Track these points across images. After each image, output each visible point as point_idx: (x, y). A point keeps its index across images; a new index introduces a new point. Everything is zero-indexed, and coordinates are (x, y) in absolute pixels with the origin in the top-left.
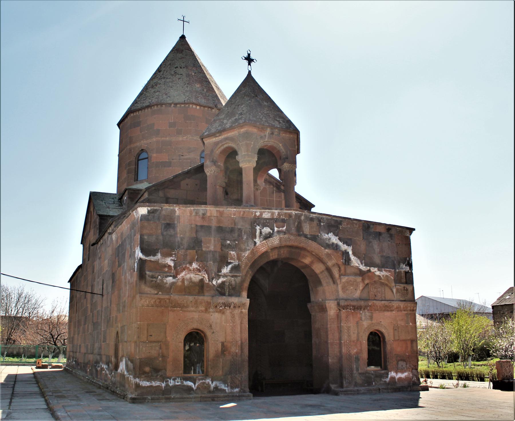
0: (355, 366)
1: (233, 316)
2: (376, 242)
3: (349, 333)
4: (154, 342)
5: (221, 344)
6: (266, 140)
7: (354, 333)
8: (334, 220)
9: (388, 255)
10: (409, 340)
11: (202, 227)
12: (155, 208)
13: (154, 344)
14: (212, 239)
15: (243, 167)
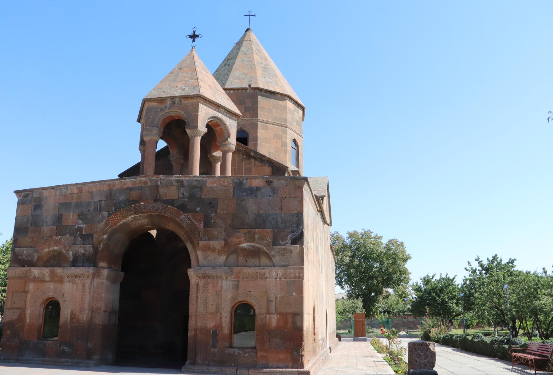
0: (211, 342)
1: (84, 286)
2: (251, 199)
3: (207, 304)
4: (17, 308)
5: (70, 311)
6: (167, 111)
7: (212, 304)
8: (195, 180)
9: (267, 213)
10: (289, 313)
11: (63, 204)
12: (28, 192)
13: (16, 311)
14: (71, 214)
15: (147, 140)
